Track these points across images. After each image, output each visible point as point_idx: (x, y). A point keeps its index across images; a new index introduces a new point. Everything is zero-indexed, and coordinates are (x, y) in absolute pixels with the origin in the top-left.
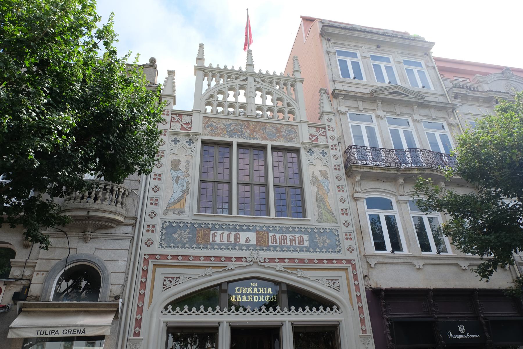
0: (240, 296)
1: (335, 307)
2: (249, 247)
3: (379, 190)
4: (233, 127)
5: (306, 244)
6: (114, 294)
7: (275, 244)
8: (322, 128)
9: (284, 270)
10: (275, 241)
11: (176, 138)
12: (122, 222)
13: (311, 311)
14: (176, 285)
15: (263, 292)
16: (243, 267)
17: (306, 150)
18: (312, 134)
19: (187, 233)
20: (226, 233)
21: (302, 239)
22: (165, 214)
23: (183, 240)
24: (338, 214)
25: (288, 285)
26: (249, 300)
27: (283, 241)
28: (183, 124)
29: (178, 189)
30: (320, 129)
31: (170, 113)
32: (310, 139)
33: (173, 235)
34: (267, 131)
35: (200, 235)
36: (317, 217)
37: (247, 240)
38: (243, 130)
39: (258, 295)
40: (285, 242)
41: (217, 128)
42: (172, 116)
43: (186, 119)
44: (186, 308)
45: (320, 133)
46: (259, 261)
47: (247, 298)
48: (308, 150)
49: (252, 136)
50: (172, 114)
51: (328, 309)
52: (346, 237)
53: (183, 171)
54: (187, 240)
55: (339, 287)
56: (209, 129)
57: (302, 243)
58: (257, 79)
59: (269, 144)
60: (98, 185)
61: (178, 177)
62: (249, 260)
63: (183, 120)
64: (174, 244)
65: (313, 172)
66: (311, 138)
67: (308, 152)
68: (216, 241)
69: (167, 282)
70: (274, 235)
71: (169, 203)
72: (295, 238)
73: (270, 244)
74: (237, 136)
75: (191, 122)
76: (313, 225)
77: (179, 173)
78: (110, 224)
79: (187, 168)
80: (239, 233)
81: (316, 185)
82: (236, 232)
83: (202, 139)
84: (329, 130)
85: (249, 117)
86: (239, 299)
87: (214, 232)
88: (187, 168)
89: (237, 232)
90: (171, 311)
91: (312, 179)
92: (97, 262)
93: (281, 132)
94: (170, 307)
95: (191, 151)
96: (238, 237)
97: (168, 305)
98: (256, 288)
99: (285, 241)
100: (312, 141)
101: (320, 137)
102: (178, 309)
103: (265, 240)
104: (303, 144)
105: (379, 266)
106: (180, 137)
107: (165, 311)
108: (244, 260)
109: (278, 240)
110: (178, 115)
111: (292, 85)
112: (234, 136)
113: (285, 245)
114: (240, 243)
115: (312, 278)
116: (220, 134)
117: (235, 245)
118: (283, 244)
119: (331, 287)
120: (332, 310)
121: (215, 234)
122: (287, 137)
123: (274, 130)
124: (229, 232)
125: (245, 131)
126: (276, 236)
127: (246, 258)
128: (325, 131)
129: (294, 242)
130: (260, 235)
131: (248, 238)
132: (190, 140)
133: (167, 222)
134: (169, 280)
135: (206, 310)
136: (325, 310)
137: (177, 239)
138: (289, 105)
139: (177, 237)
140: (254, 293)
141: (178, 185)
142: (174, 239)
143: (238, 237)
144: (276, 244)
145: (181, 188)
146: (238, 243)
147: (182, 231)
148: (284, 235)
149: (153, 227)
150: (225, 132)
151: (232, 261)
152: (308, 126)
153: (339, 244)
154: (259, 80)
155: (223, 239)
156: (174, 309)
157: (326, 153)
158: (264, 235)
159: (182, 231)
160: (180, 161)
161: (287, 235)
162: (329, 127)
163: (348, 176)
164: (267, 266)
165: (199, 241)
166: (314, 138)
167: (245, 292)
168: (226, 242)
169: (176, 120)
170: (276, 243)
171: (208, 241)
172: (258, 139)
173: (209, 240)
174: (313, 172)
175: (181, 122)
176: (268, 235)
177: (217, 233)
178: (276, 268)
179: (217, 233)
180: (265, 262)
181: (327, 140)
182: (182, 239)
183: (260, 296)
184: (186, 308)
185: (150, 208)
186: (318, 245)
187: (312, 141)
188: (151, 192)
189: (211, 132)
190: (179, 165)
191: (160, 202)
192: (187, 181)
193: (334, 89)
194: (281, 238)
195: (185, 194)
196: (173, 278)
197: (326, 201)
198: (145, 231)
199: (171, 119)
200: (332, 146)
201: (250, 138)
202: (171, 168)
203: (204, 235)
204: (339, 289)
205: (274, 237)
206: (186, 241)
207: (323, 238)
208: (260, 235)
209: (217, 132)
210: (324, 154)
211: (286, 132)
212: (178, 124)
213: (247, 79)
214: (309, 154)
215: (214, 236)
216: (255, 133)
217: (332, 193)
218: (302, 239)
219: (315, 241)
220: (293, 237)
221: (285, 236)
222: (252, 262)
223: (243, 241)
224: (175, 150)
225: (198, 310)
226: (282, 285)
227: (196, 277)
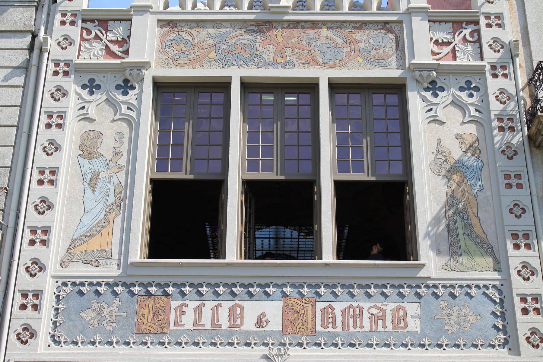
2: (265, 337)
4: (234, 41)
5: (413, 326)
7: (330, 329)
8: (468, 23)
10: (331, 320)
11: (92, 80)
17: (422, 84)
18: (440, 41)
19: (114, 308)
20: (209, 305)
21: (402, 314)
22: (63, 264)
23: (105, 325)
27: (352, 320)
28: (109, 44)
29: (97, 203)
30: (464, 25)
32: (434, 54)
33: (82, 314)
34: (321, 42)
35: (146, 312)
37: (261, 321)
38: (258, 45)
40: (358, 324)
41: (193, 46)
42: (85, 25)
45: (462, 35)
48: (426, 85)
49: (280, 59)
50: (84, 21)
52: (523, 306)
54: (115, 324)
56: (171, 52)
57: (402, 325)
61: (96, 174)
63: (108, 34)
64: (84, 335)
65: (439, 140)
67: (427, 89)
68: (183, 326)
70: (330, 306)
71: (74, 238)
72: (383, 311)
73: (318, 328)
74: (242, 62)
75: (129, 37)
76: (433, 276)
77: (97, 164)
79: (118, 150)
80: (240, 303)
82: (232, 303)
83: (154, 78)
84: (489, 26)
87: (180, 302)
88: (118, 150)
89: (237, 301)
91: (435, 158)
93: (357, 42)
95: (129, 108)
96: (238, 312)
99: (358, 320)
100: (437, 60)
103: (307, 319)
104: (413, 71)
106: (101, 76)
109: (339, 318)
110: (97, 23)
112: (234, 63)
113: (358, 329)
114: (242, 328)
116: (199, 61)
117: (231, 333)
118: (352, 329)
121: (181, 309)
122: (373, 53)
123: (338, 40)
124: (216, 303)
125: (262, 49)
126: (333, 309)
128: (478, 31)
129: (380, 322)
130: (292, 306)
131: (263, 315)
132: (126, 81)
133: (69, 284)
137: (90, 324)
139: (92, 319)
142: (84, 322)
143: (238, 312)
144: (333, 330)
145: (103, 202)
146: (237, 329)
147: (103, 304)
148: (355, 304)
149: (37, 296)
150: (213, 55)
152: (430, 21)
153: (503, 326)
155: (200, 320)
158: (303, 307)
159: (103, 304)
161: (361, 304)
162: (488, 17)
163: (537, 144)
165: (143, 327)
168: (208, 326)
169: (93, 35)
170: (334, 327)
171: (163, 325)
172: (296, 66)
173: (168, 324)
174: (439, 140)
175: (104, 38)
176: (313, 306)
177: (186, 306)
179: (186, 306)
181: (481, 53)
182: (105, 322)
186: (446, 328)
187: (437, 60)
189: (178, 57)
190: (99, 145)
191: (54, 238)
192: (116, 182)
194: (348, 312)
195: (112, 215)
197: (471, 215)
198: (17, 306)
199: (82, 33)
201: (274, 65)
202: (81, 152)
203: (156, 313)
205: (330, 310)
206: (113, 327)
207: (459, 311)
209: (193, 56)
211: (371, 41)
214: (428, 95)
215: (180, 312)
216: (289, 52)
217: (489, 193)
218: (402, 314)
219: (436, 317)
220: (379, 308)
221: (358, 306)
223: (249, 323)
224: (92, 111)
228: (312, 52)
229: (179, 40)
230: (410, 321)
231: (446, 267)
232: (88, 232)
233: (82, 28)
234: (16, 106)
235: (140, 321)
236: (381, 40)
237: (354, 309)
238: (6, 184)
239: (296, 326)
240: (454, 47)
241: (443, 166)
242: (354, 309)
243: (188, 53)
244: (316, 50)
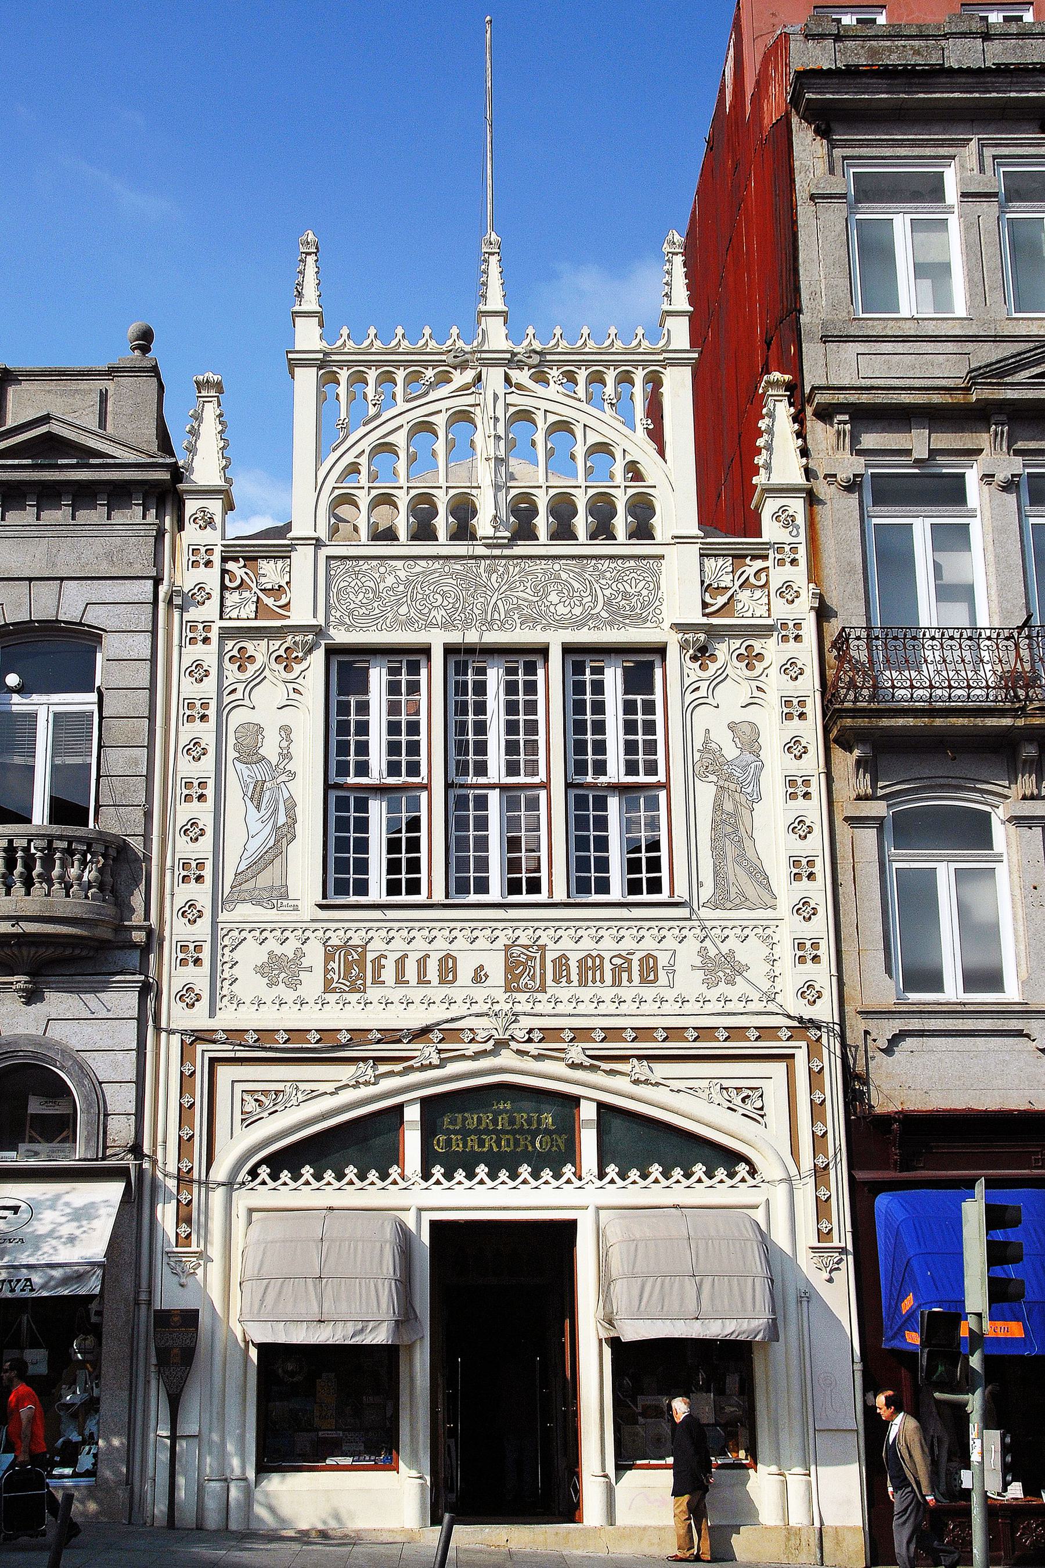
0: (459, 1137)
1: (742, 1169)
3: (942, 781)
6: (114, 1140)
8: (754, 557)
9: (588, 1062)
10: (564, 973)
12: (110, 941)
13: (667, 1179)
14: (276, 1111)
15: (526, 1127)
16: (463, 1057)
24: (779, 873)
25: (601, 1106)
26: (485, 1150)
27: (590, 973)
31: (216, 558)
32: (705, 605)
35: (336, 966)
36: (707, 892)
39: (513, 1132)
40: (598, 978)
43: (270, 572)
44: (307, 1171)
46: (513, 1038)
47: (481, 1144)
50: (224, 560)
51: (721, 1173)
53: (274, 763)
55: (761, 1109)
57: (652, 977)
58: (516, 375)
59: (555, 640)
60: (30, 841)
62: (481, 1035)
65: (708, 731)
66: (708, 599)
67: (694, 658)
69: (251, 1106)
77: (258, 772)
78: (77, 952)
81: (715, 779)
84: (781, 562)
85: (487, 546)
86: (458, 1146)
90: (268, 1180)
92: (59, 1057)
94: (264, 1171)
96: (450, 965)
97: (258, 1165)
98: (504, 1116)
101: (744, 596)
102: (285, 1175)
105: (909, 1043)
107: (252, 1181)
108: (467, 1036)
110: (242, 562)
111: (655, 381)
115: (676, 1085)
119: (735, 1111)
120: (731, 1175)
127: (471, 1030)
129: (625, 975)
130: (519, 956)
131: (481, 967)
134: (256, 1100)
135: (362, 1177)
136: (711, 1177)
138: (634, 471)
140: (500, 1127)
141: (263, 812)
143: (450, 965)
151: (431, 1041)
152: (701, 555)
154: (522, 376)
156: (275, 1177)
157: (760, 657)
160: (259, 729)
161: (602, 953)
164: (535, 1052)
165: (334, 985)
166: (721, 600)
167: (472, 1127)
174: (708, 731)
175: (253, 585)
176: (543, 958)
178: (562, 1059)
180: (530, 1040)
181: (769, 604)
183: (517, 1136)
184: (307, 1171)
185: (185, 893)
188: (182, 841)
192: (286, 795)
193: (813, 388)
196: (264, 1092)
197: (745, 835)
200: (784, 626)
203: (348, 966)
204: (762, 1116)
208: (519, 956)
210: (751, 659)
212: (246, 594)
213: (479, 378)
221: (599, 956)
222: (492, 1042)
225: (340, 1176)
226: (583, 1103)
227: (330, 1087)
228: (540, 603)
229: (356, 588)
230: (662, 974)
231: (708, 905)
232: (256, 863)
233: (224, 572)
234: (145, 689)
235: (329, 978)
236: (633, 585)
237: (593, 958)
238: (144, 800)
239: (521, 981)
240: (732, 596)
241: (710, 768)
242: (593, 958)
243: (370, 607)
244: (545, 600)
